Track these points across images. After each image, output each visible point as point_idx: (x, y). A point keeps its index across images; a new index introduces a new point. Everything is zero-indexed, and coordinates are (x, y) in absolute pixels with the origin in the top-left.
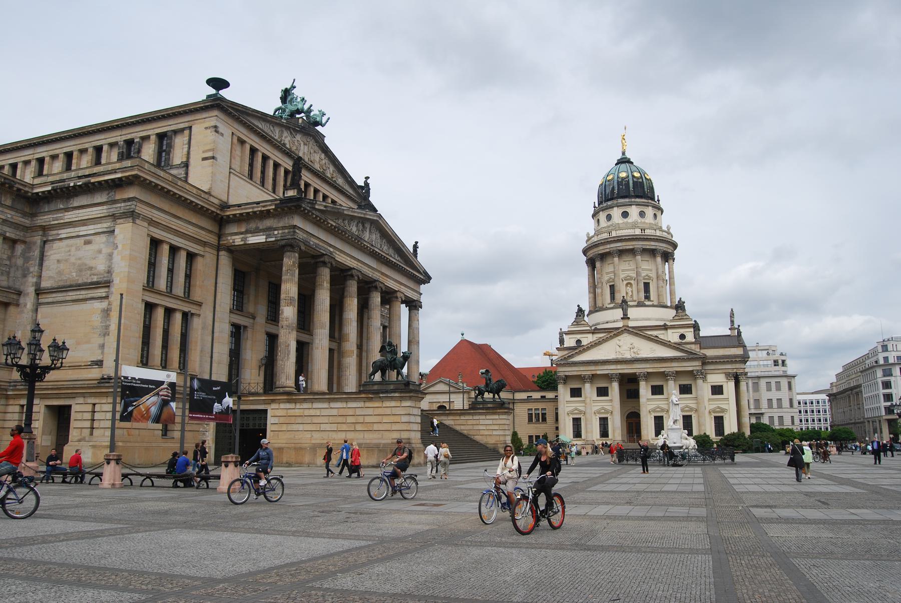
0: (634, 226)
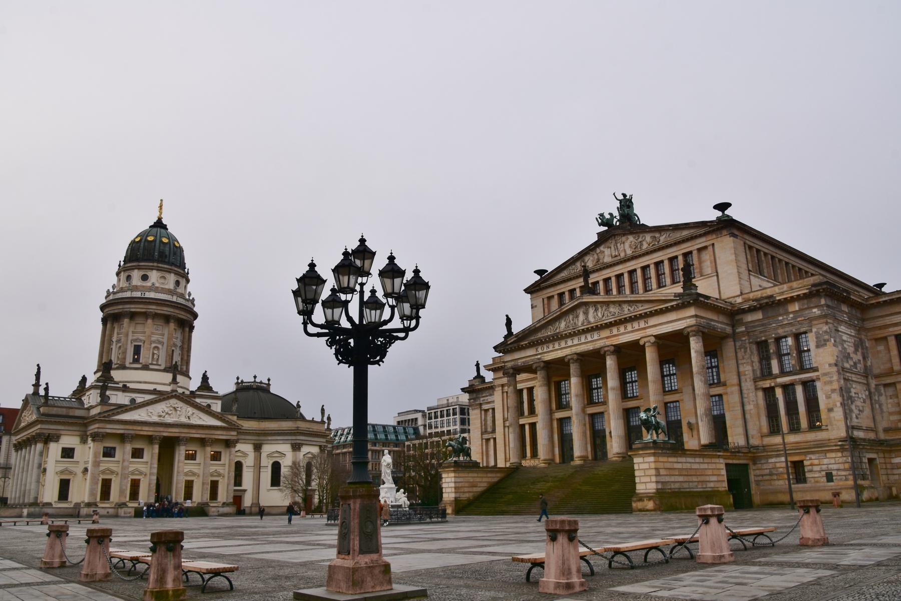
0: (170, 292)
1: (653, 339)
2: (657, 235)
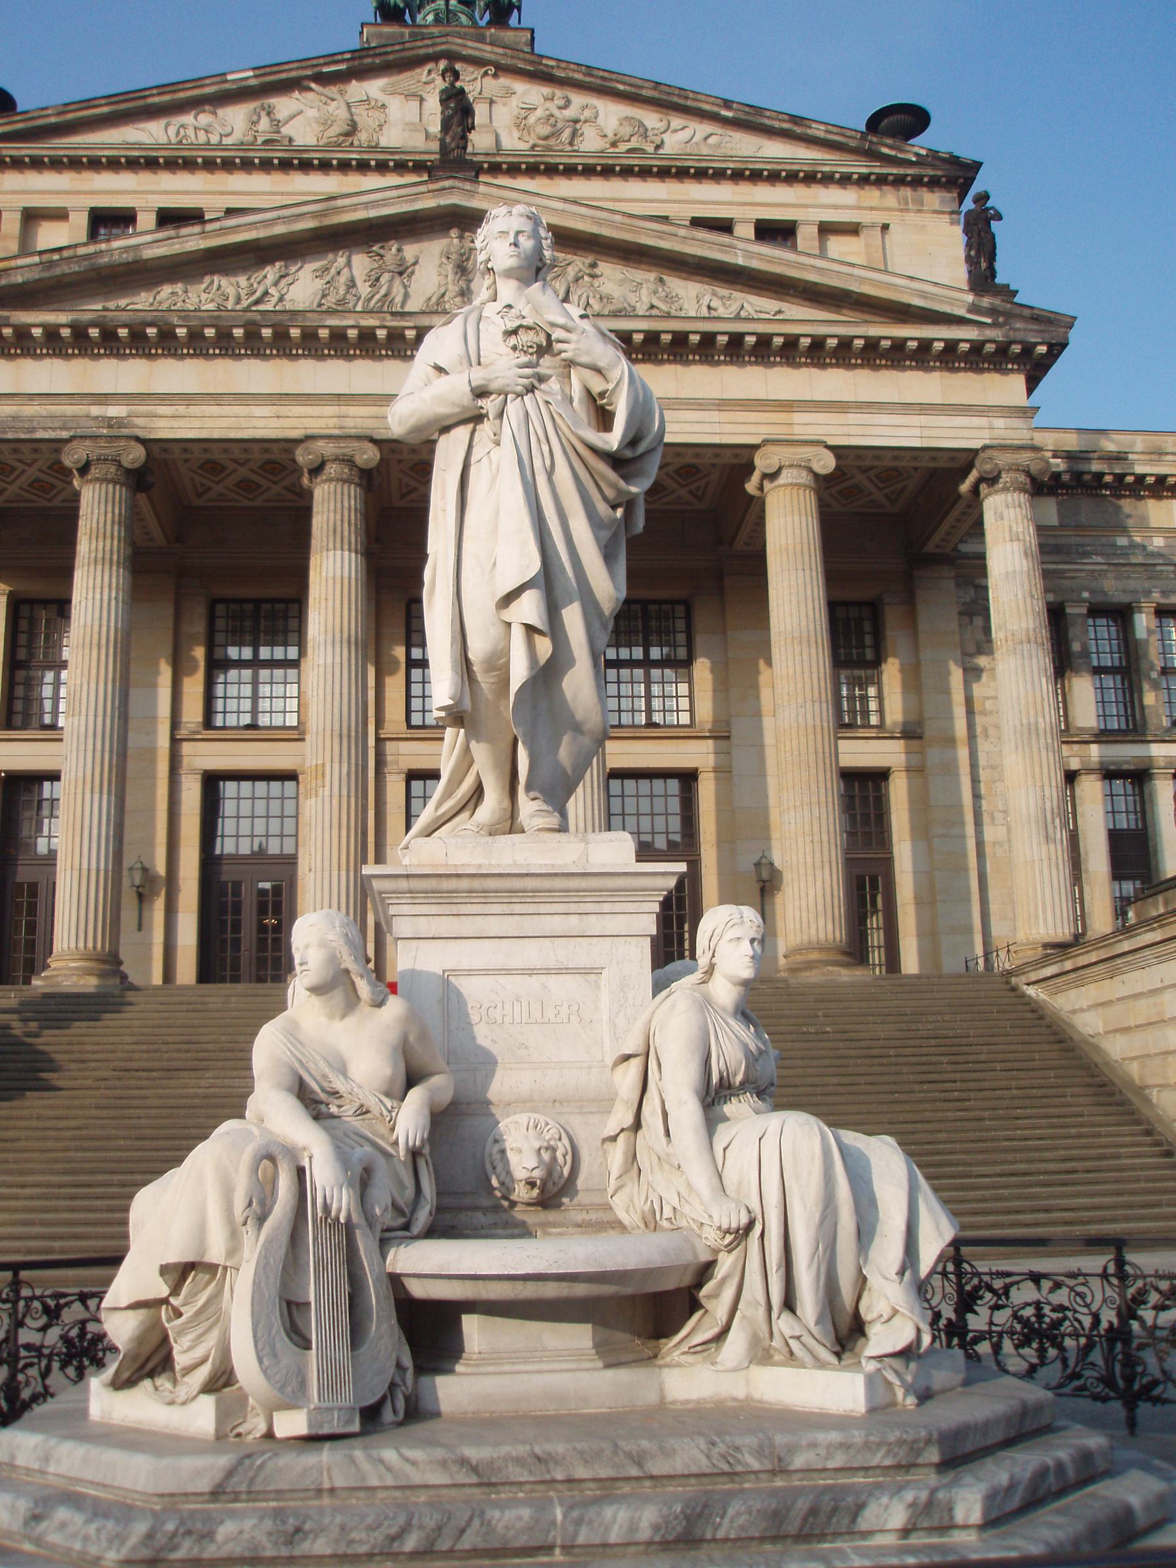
1: (826, 463)
2: (651, 119)
